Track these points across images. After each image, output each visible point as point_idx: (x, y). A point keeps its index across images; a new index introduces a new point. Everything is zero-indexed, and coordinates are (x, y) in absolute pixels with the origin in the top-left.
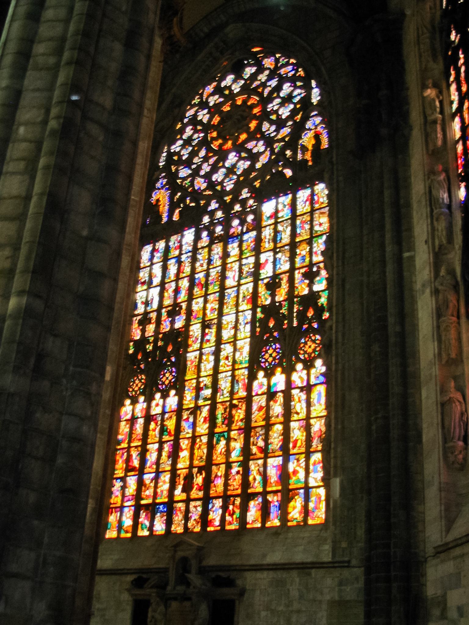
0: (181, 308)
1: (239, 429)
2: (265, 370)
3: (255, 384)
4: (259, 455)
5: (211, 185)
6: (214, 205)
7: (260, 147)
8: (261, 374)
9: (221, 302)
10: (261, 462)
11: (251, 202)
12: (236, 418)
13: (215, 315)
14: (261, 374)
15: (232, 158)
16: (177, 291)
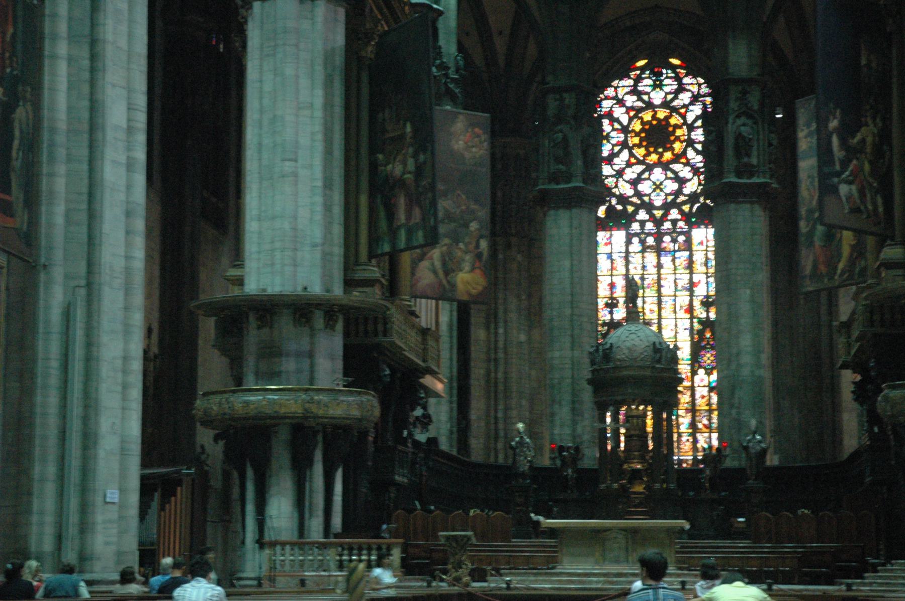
0: (618, 301)
1: (686, 409)
2: (705, 368)
3: (696, 378)
4: (704, 430)
5: (638, 194)
6: (642, 215)
7: (685, 172)
8: (701, 372)
9: (660, 303)
10: (707, 435)
11: (681, 224)
12: (682, 401)
13: (655, 316)
14: (701, 372)
15: (658, 174)
16: (612, 286)
